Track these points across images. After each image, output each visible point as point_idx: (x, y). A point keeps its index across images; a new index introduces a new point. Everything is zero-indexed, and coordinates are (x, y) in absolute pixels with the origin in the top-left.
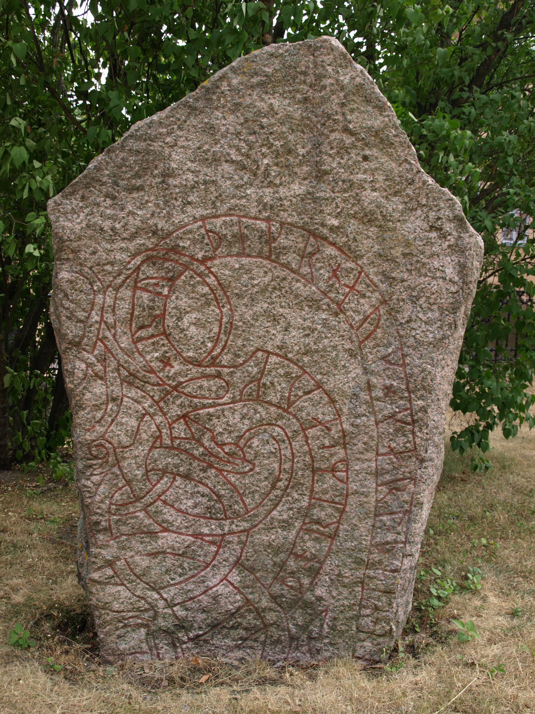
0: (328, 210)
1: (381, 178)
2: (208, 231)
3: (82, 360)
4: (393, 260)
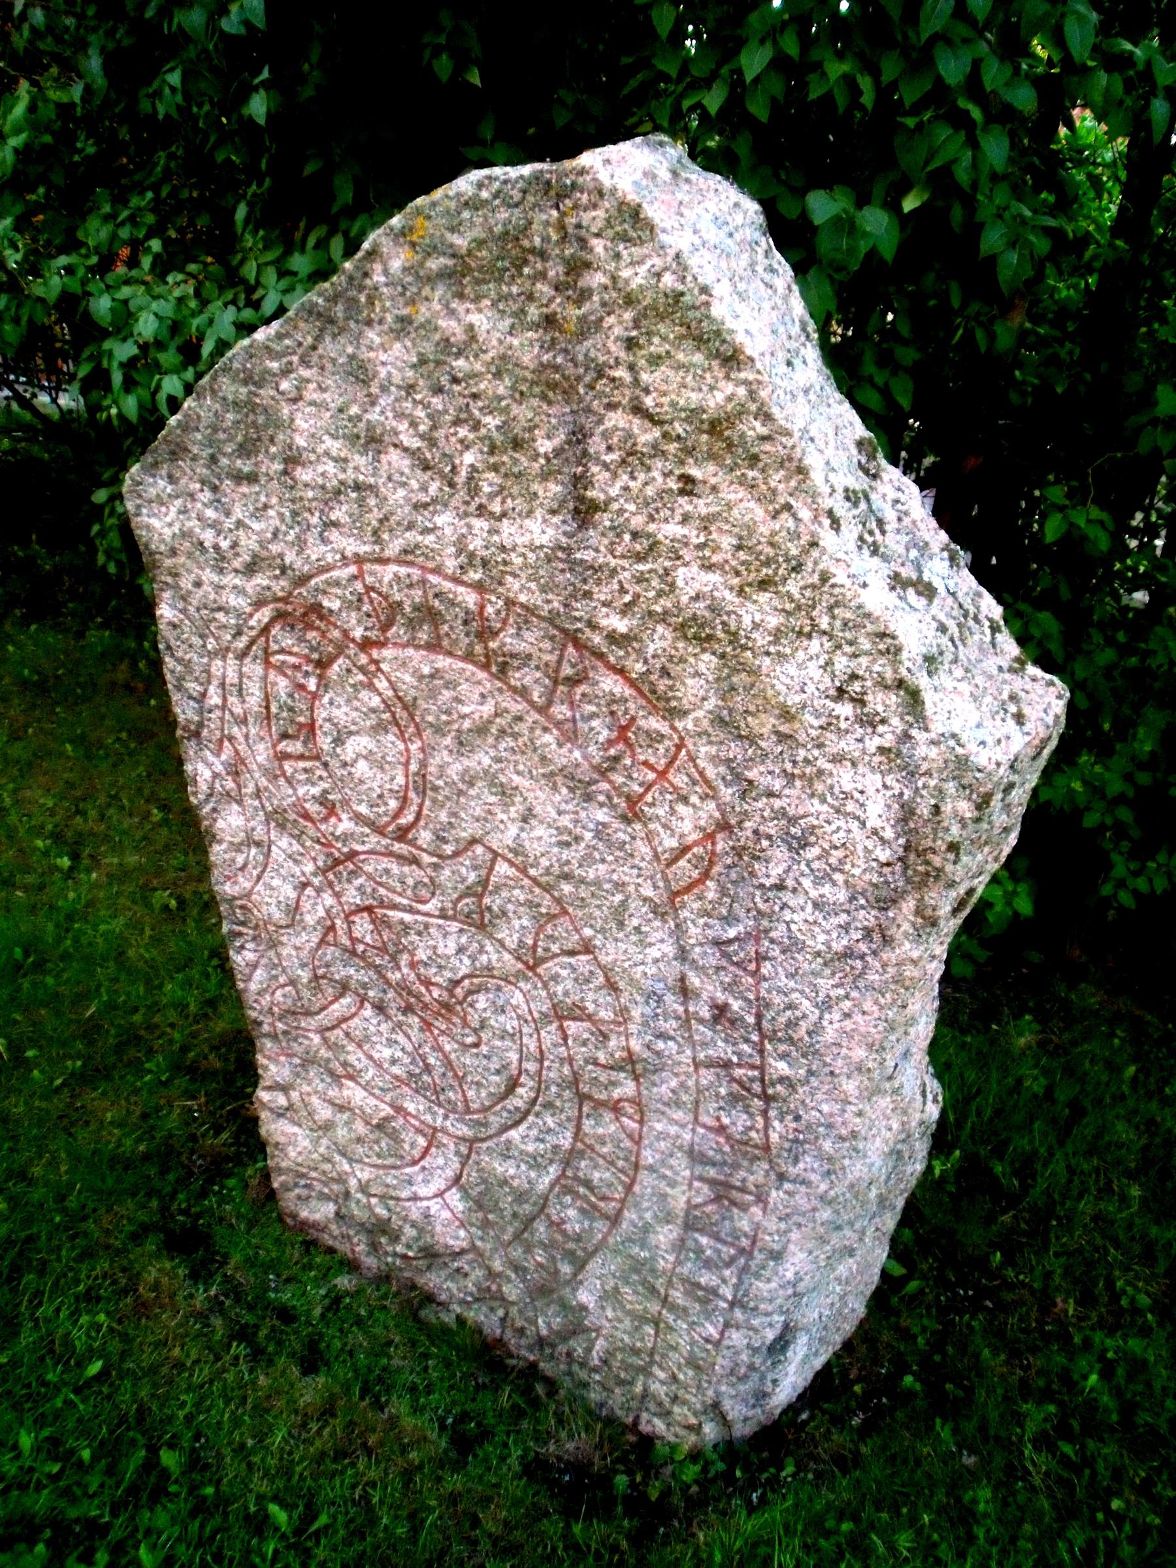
0: (602, 593)
1: (727, 542)
4: (752, 739)
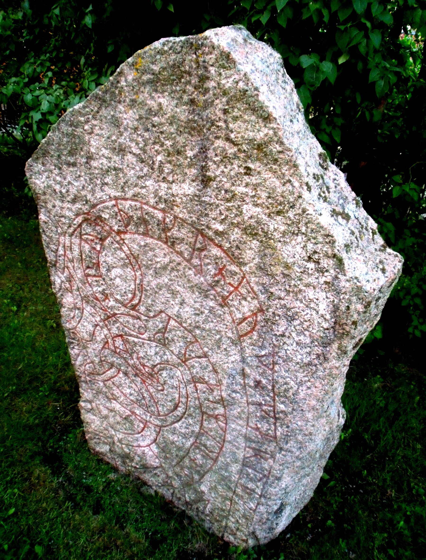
1: (264, 195)
4: (273, 276)
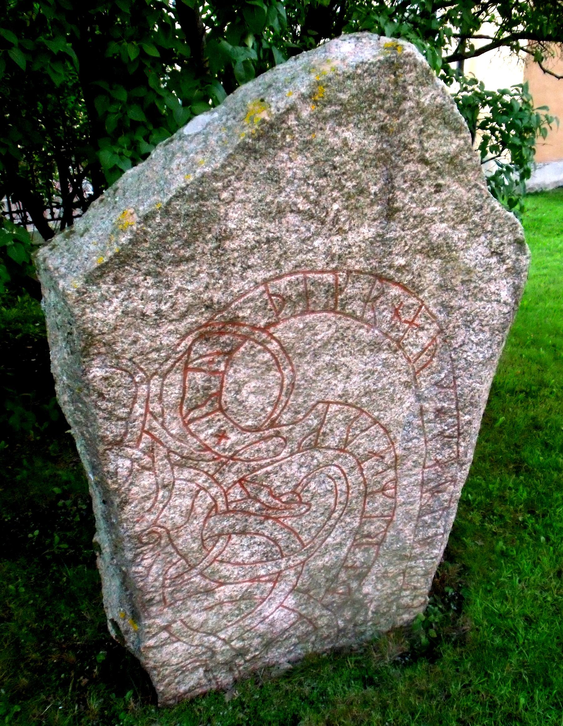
0: (395, 250)
1: (450, 208)
2: (270, 295)
3: (126, 457)
